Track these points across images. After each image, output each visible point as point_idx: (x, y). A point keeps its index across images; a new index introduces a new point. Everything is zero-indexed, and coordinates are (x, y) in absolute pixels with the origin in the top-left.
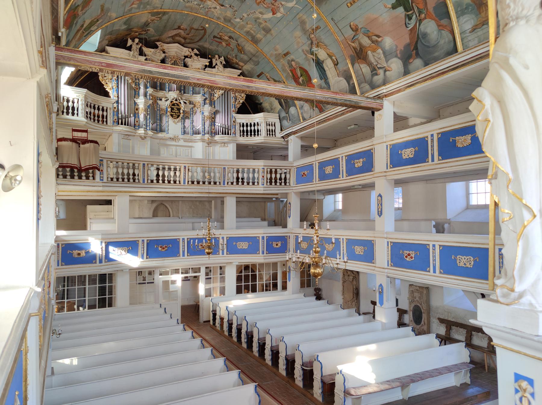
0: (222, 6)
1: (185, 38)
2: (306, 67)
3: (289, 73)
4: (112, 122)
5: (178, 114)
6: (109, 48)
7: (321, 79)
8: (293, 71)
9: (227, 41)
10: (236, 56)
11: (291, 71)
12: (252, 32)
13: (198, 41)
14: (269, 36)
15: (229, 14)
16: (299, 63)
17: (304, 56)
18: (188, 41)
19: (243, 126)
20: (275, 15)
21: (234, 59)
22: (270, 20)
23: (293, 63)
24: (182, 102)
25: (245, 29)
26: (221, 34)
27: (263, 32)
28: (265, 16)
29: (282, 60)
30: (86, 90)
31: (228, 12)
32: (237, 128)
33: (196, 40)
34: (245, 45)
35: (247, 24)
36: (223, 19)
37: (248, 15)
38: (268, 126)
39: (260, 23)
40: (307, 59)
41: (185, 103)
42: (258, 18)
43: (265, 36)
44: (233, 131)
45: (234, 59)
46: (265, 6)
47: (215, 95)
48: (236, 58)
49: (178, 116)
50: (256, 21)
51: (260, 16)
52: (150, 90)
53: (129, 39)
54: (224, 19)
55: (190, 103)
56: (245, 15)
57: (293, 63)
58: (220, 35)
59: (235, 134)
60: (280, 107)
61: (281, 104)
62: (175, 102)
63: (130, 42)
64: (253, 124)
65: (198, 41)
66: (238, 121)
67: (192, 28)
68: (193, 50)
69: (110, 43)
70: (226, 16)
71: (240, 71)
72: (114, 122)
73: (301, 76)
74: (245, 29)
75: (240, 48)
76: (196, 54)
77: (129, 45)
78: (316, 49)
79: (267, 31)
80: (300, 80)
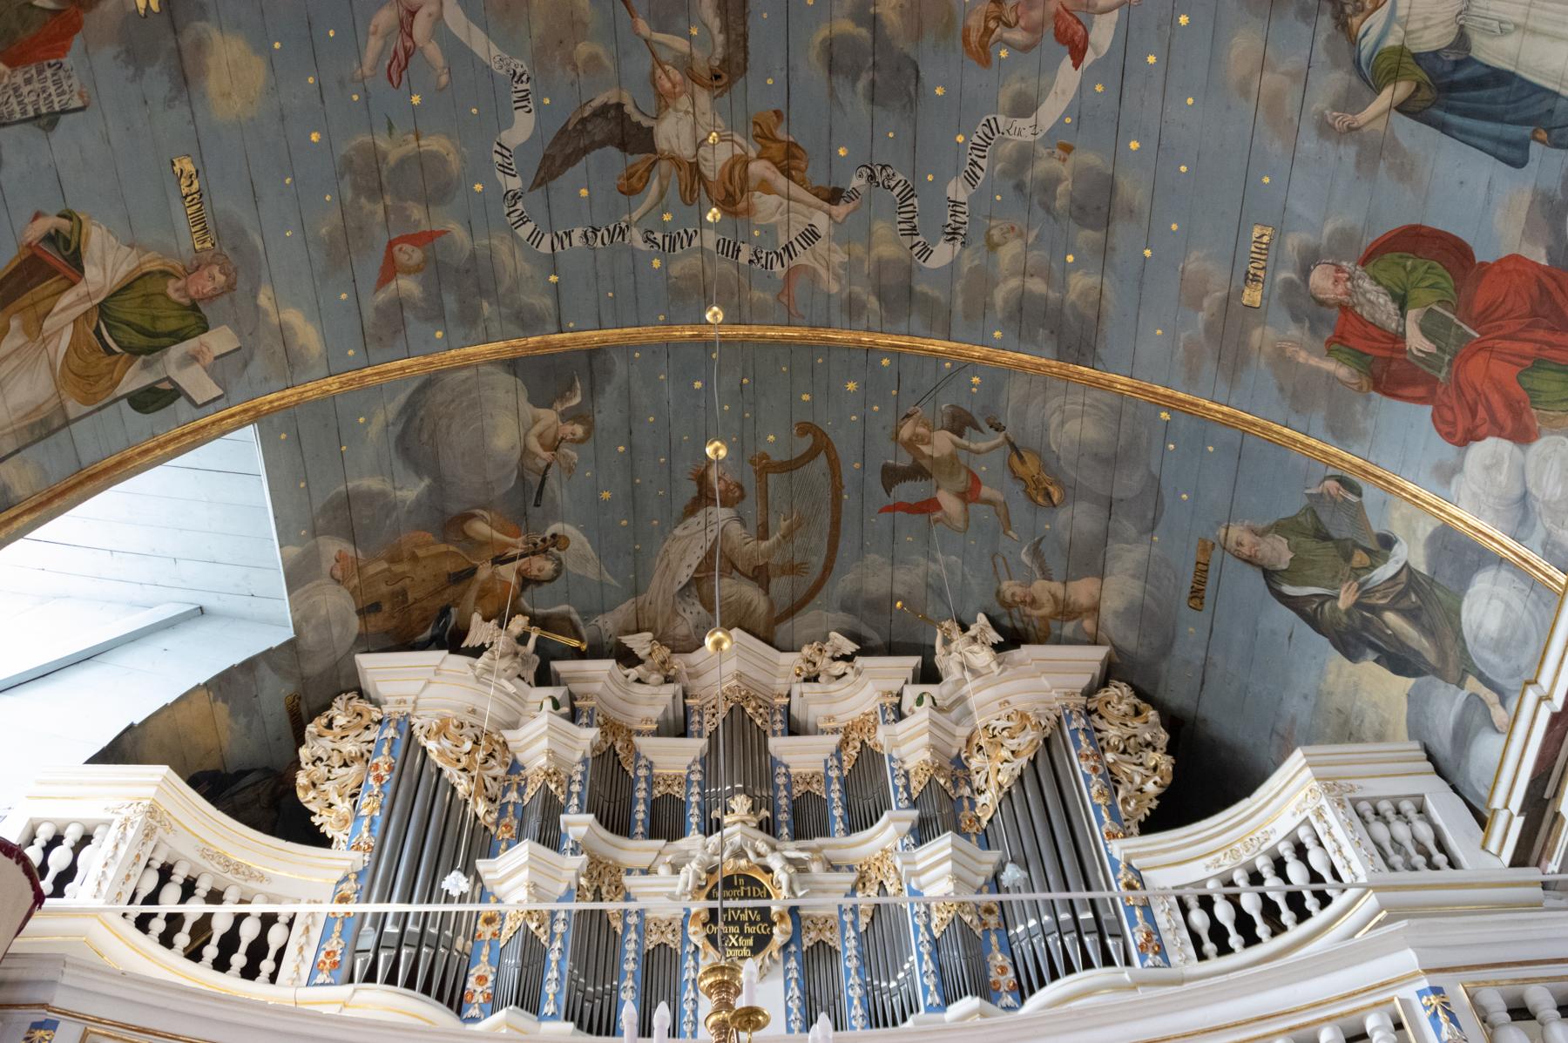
0: (834, 196)
1: (760, 576)
2: (1398, 213)
3: (1331, 377)
4: (305, 971)
5: (761, 929)
6: (376, 668)
7: (1515, 155)
8: (1347, 331)
9: (951, 463)
10: (1036, 552)
11: (1337, 344)
12: (1037, 286)
13: (828, 568)
14: (1122, 232)
15: (887, 244)
16: (1345, 238)
17: (1349, 152)
18: (781, 586)
19: (1206, 903)
20: (1089, 57)
21: (1042, 588)
22: (1079, 111)
23: (1321, 280)
24: (775, 862)
25: (1000, 295)
26: (906, 432)
27: (1086, 236)
28: (1052, 110)
29: (1256, 335)
30: (164, 769)
31: (881, 228)
32: (1162, 920)
33: (817, 562)
34: (1045, 427)
35: (993, 247)
36: (873, 303)
37: (971, 178)
38: (1380, 830)
39: (1049, 185)
40: (1375, 152)
41: (799, 866)
42: (1025, 156)
43: (1105, 251)
44: (1135, 937)
45: (1041, 588)
46: (1017, 36)
47: (981, 800)
48: (1047, 577)
49: (761, 943)
50: (1019, 187)
51: (1023, 130)
52: (578, 824)
53: (476, 618)
54: (880, 298)
55: (833, 867)
56: (958, 190)
57: (1321, 280)
58: (910, 445)
59: (1161, 950)
60: (1406, 683)
61: (1400, 661)
62: (730, 867)
63: (479, 631)
64: (1264, 866)
65: (828, 568)
66: (1163, 879)
67: (765, 467)
68: (826, 639)
69: (377, 622)
70: (881, 265)
71: (1099, 653)
72: (316, 968)
73: (1402, 303)
74: (1000, 295)
75: (1031, 467)
76: (847, 658)
77: (471, 640)
78: (1379, 18)
79: (1099, 206)
80: (1416, 341)
